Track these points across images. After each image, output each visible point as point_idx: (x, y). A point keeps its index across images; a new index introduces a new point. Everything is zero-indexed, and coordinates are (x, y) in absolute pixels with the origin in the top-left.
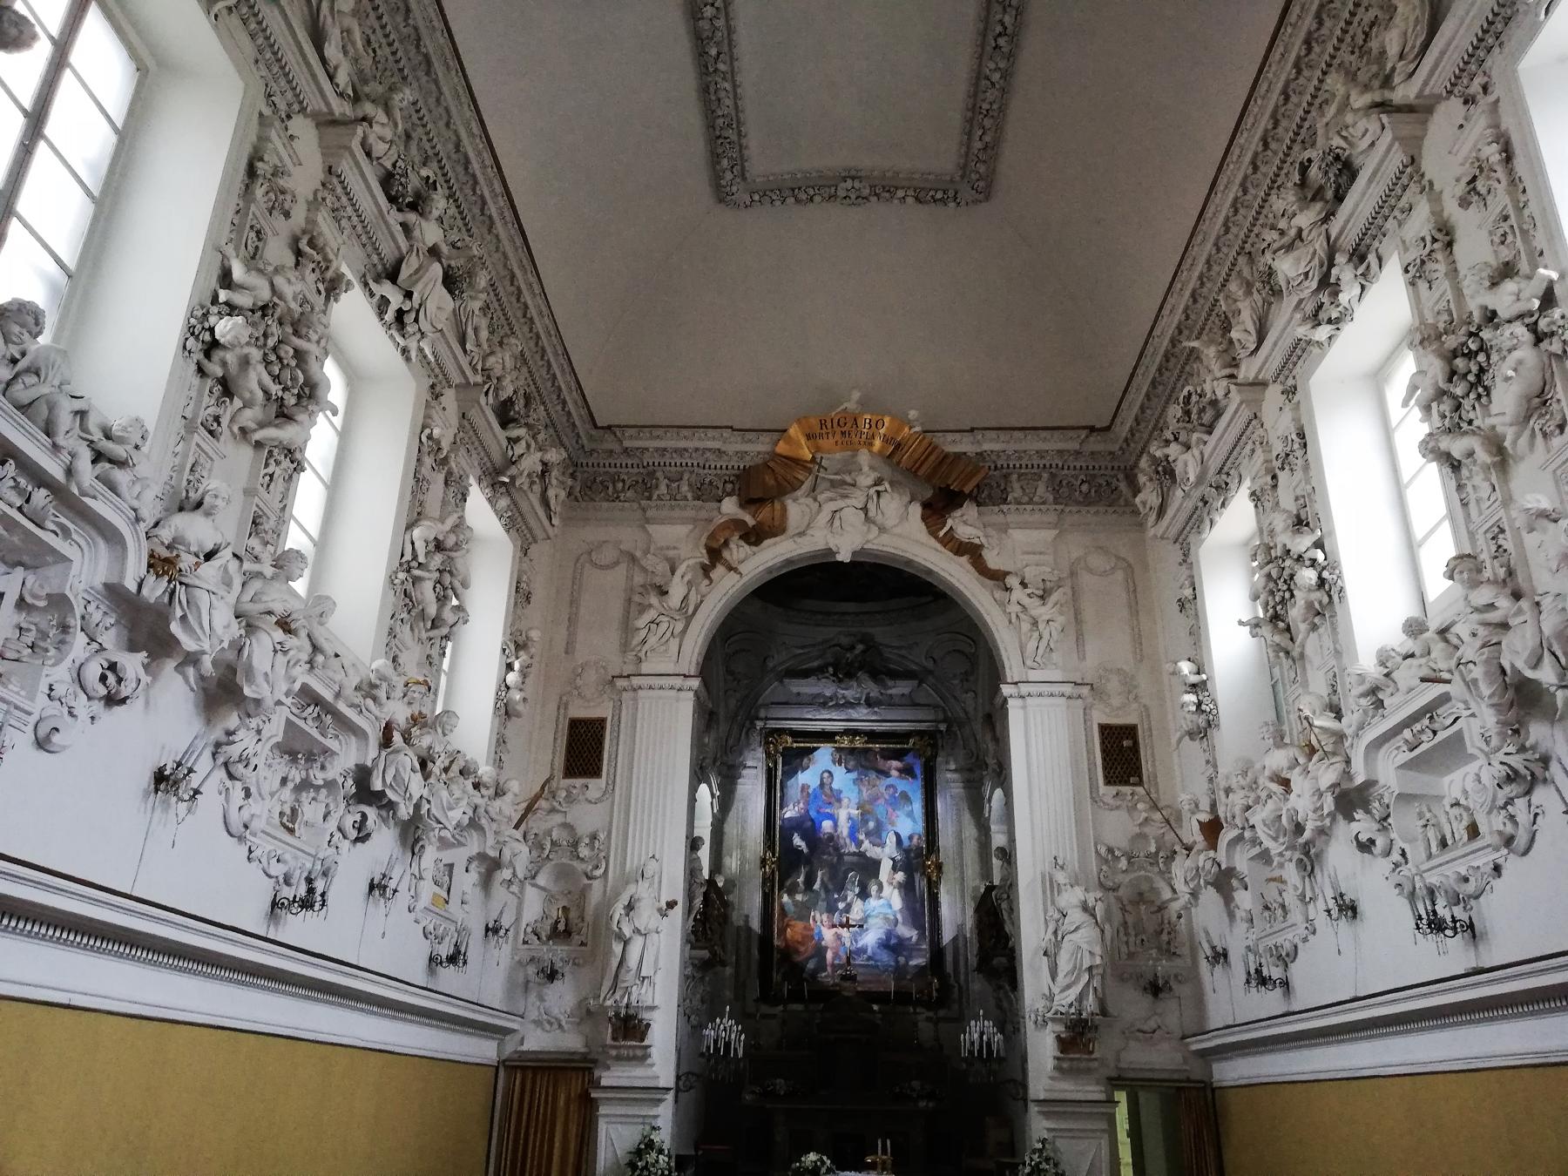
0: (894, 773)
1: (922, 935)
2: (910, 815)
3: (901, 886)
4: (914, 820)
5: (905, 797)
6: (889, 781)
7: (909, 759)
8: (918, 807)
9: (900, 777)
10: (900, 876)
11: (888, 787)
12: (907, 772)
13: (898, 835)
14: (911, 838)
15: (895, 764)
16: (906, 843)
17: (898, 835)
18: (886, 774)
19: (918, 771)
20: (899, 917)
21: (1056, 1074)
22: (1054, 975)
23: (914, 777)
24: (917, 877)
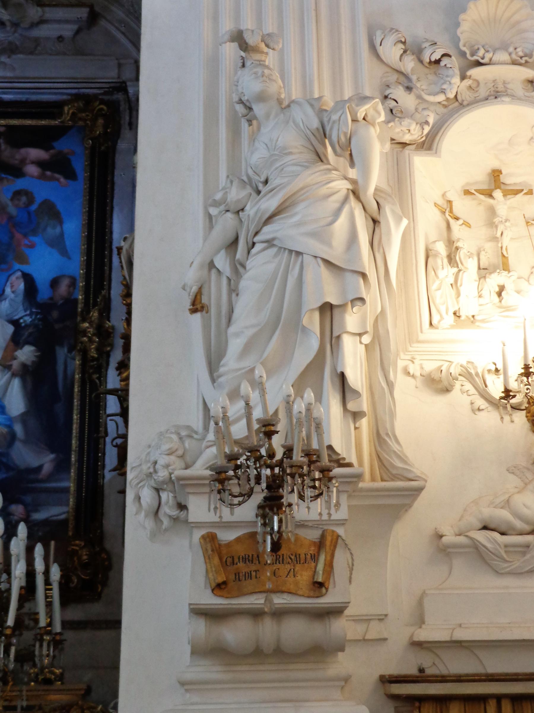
0: (32, 170)
1: (62, 466)
2: (58, 243)
3: (26, 373)
4: (64, 252)
5: (51, 211)
6: (20, 184)
7: (64, 145)
8: (73, 228)
9: (43, 177)
10: (26, 354)
11: (17, 194)
12: (59, 166)
13: (28, 279)
14: (55, 283)
15: (35, 153)
16: (44, 294)
17: (28, 279)
18: (17, 172)
19: (80, 165)
20: (18, 429)
21: (209, 670)
22: (213, 364)
23: (71, 175)
24: (61, 353)
